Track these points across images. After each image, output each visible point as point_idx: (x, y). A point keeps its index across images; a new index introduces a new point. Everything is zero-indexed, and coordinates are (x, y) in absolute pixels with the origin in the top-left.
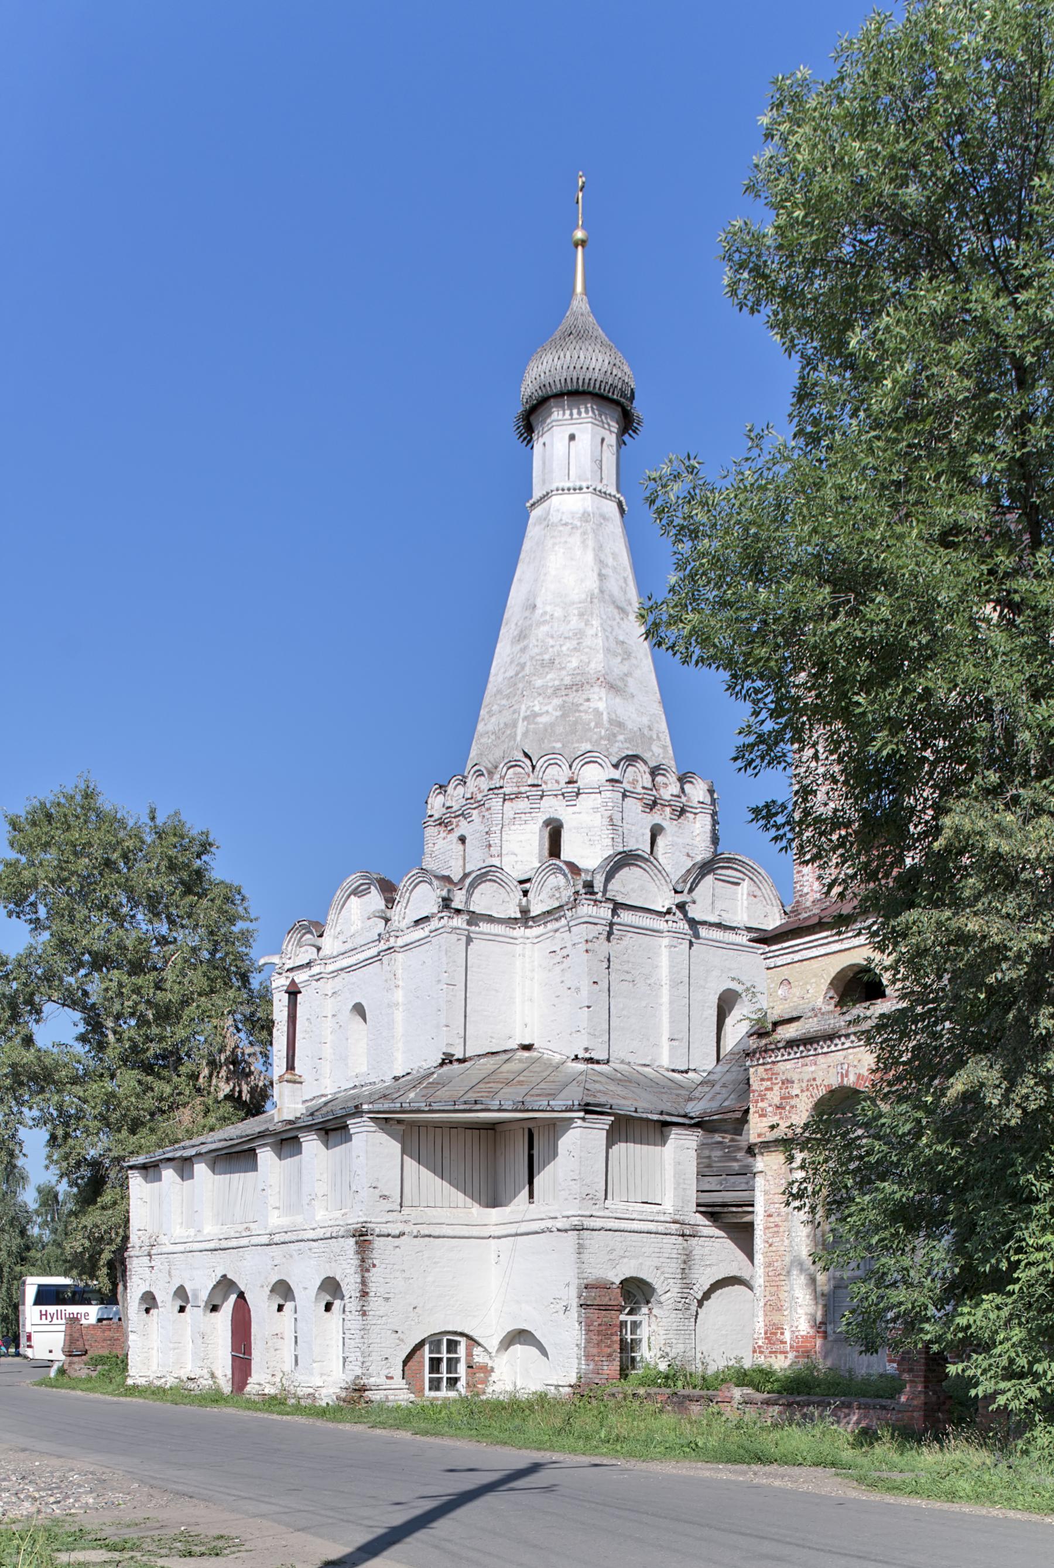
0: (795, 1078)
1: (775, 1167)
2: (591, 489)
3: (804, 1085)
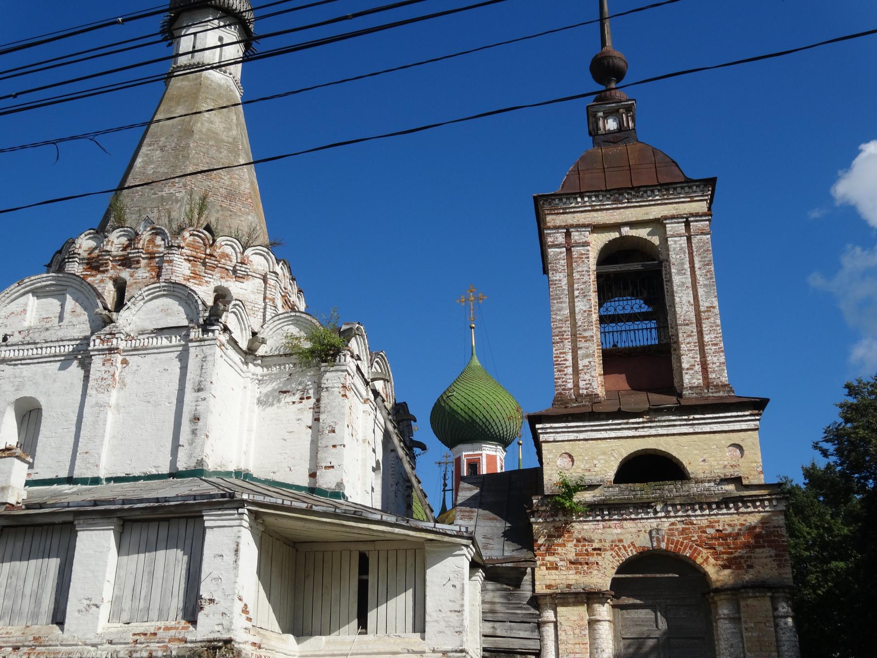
0: (595, 537)
1: (575, 618)
2: (231, 76)
3: (607, 545)
